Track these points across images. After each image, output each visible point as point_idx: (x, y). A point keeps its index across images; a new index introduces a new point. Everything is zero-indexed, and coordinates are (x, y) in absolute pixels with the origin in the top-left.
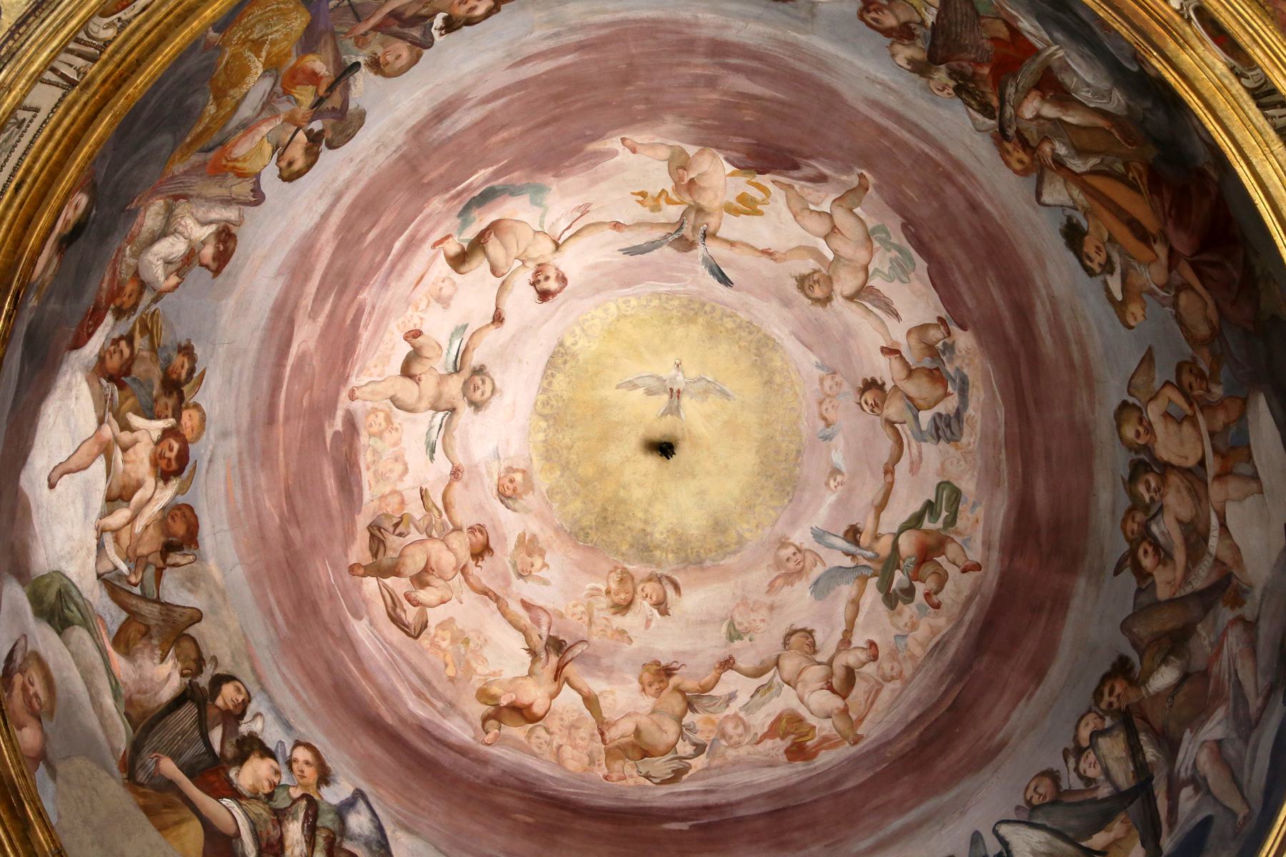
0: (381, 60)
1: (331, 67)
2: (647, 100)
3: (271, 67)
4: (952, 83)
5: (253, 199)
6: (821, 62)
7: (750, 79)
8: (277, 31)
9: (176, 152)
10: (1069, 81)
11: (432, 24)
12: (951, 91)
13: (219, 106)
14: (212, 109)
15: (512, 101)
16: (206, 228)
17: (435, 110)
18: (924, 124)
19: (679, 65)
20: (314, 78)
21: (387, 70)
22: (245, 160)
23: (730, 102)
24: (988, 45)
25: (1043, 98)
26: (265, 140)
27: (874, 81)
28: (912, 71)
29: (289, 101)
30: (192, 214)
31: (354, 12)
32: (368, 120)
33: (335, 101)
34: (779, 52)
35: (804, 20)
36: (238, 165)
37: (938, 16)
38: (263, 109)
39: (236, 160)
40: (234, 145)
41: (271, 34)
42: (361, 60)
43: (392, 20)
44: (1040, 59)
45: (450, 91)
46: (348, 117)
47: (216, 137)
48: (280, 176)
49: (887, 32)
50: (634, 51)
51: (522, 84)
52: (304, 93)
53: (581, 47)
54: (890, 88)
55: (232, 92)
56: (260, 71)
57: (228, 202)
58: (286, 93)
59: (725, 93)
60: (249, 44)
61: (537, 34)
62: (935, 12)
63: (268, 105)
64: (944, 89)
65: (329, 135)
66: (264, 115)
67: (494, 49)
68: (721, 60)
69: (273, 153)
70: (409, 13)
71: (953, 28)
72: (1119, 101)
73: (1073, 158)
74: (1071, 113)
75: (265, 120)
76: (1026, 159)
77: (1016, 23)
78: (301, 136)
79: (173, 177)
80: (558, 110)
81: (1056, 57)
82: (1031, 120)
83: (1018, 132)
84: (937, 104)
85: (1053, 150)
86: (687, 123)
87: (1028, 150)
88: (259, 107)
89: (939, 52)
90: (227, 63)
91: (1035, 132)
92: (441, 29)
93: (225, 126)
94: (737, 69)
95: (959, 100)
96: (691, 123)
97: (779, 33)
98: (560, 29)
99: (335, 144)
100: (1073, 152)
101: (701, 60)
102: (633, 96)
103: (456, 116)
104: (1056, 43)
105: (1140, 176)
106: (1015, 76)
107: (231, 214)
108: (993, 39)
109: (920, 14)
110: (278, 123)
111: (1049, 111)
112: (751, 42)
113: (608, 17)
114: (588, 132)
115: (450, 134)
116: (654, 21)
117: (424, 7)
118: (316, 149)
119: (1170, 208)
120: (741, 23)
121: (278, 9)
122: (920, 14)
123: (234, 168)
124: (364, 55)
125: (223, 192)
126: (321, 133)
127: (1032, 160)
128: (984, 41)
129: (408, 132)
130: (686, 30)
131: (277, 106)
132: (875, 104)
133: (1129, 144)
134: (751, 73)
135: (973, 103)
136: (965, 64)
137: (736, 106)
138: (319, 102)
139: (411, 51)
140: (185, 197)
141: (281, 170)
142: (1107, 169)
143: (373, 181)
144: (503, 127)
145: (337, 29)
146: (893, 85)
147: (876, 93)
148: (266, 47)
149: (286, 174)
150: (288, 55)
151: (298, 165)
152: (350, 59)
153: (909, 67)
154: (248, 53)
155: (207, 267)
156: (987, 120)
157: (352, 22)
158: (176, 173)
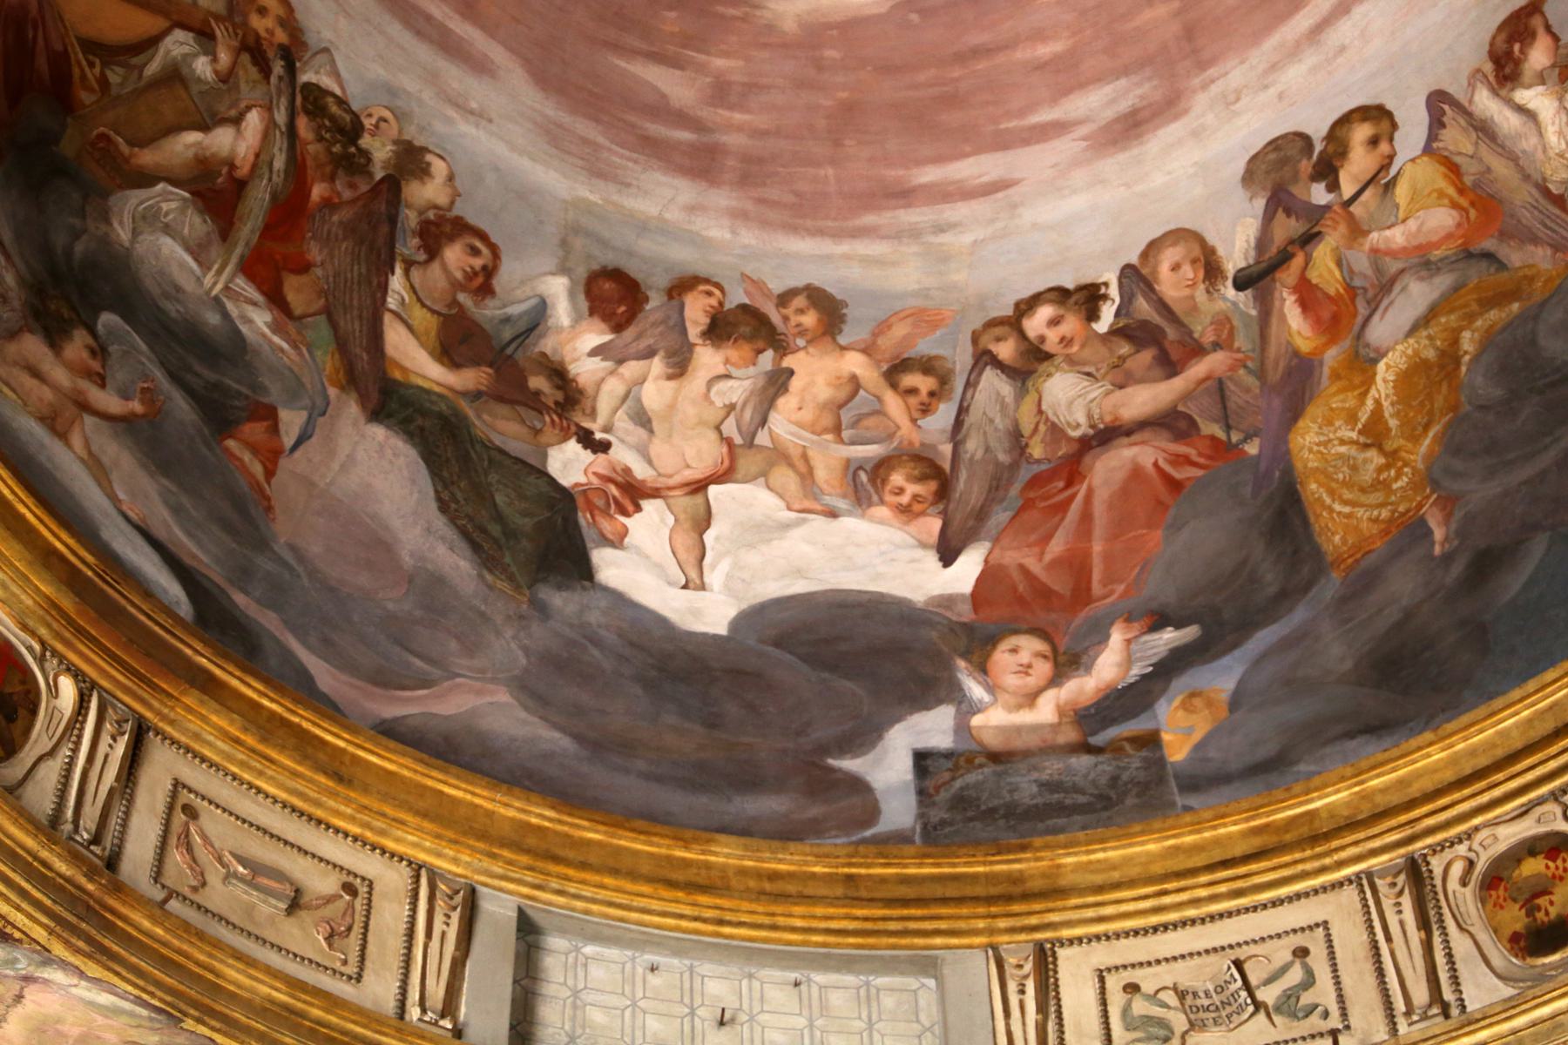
0: (1201, 274)
1: (1277, 303)
2: (819, 66)
3: (1362, 363)
4: (365, 141)
5: (1446, 107)
6: (554, 136)
7: (664, 96)
8: (1342, 442)
9: (1538, 297)
10: (196, 224)
11: (1118, 314)
12: (368, 123)
13: (1455, 342)
14: (1468, 342)
15: (1022, 113)
16: (1531, 106)
17: (1139, 136)
18: (406, 38)
19: (764, 134)
20: (1308, 295)
21: (1197, 251)
22: (1441, 194)
23: (699, 51)
24: (315, 253)
25: (232, 166)
26: (1401, 215)
27: (479, 116)
28: (424, 150)
29: (1351, 271)
30: (1545, 150)
31: (1225, 407)
32: (1240, 166)
33: (1287, 228)
34: (618, 157)
35: (577, 230)
36: (1451, 191)
37: (384, 288)
38: (1393, 281)
39: (1454, 205)
40: (1449, 236)
41: (1352, 442)
42: (1230, 292)
43: (1175, 354)
44: (238, 251)
45: (1111, 165)
46: (1269, 186)
47: (1477, 273)
48: (1394, 126)
49: (461, 228)
50: (830, 171)
51: (1003, 142)
52: (1326, 274)
53: (905, 195)
54: (457, 106)
55: (1430, 354)
56: (1381, 366)
57: (1484, 129)
58: (1352, 291)
59: (701, 69)
60: (1390, 445)
61: (967, 239)
62: (392, 302)
63: (1385, 286)
64: (377, 126)
65: (1306, 166)
66: (1393, 266)
67: (1035, 226)
68: (706, 139)
69: (1395, 178)
70: (1147, 356)
71: (364, 270)
72: (121, 223)
73: (185, 56)
74: (190, 153)
75: (1393, 254)
76: (259, 24)
77: (275, 319)
78: (1348, 190)
79: (1556, 248)
80: (956, 74)
81: (216, 267)
82: (249, 108)
83: (266, 72)
84: (392, 91)
85: (215, 60)
86: (767, 14)
87: (251, 40)
88: (1397, 288)
89: (383, 207)
90: (1427, 427)
91: (243, 86)
92: (1105, 297)
93: (1456, 289)
94: (682, 118)
95: (355, 107)
96: (758, 13)
97: (615, 198)
98: (932, 239)
99: (1300, 143)
100: (185, 71)
101: (733, 140)
102: (840, 79)
103: (1110, 114)
104: (217, 299)
105: (83, 77)
106: (274, 196)
107: (1485, 103)
108: (304, 268)
109: (412, 287)
110: (1374, 236)
111: (221, 140)
112: (659, 176)
113: (863, 247)
114: (914, 17)
115: (1123, 82)
116: (793, 229)
117: (1123, 359)
118: (1331, 149)
119: (35, 38)
120: (667, 216)
121: (1331, 493)
122: (412, 287)
123: (1461, 191)
124: (1225, 299)
125: (1485, 152)
126: (1317, 176)
127: (245, 24)
128: (319, 259)
129: (1186, 111)
130: (749, 206)
131: (1369, 272)
132: (480, 66)
133: (103, 136)
134: (662, 110)
135: (334, 109)
136: (347, 194)
137: (688, 41)
138: (1309, 239)
139: (1155, 272)
140: (1546, 193)
141: (1391, 139)
142: (135, 61)
143: (1257, 37)
144: (1041, 66)
145: (1251, 381)
146: (451, 112)
147: (477, 90)
148: (1364, 417)
149: (1385, 124)
150: (1336, 376)
151: (1361, 133)
152: (1244, 299)
153: (429, 158)
154: (1393, 423)
155: (1548, 29)
156: (314, 80)
157: (1232, 387)
158: (1549, 252)
